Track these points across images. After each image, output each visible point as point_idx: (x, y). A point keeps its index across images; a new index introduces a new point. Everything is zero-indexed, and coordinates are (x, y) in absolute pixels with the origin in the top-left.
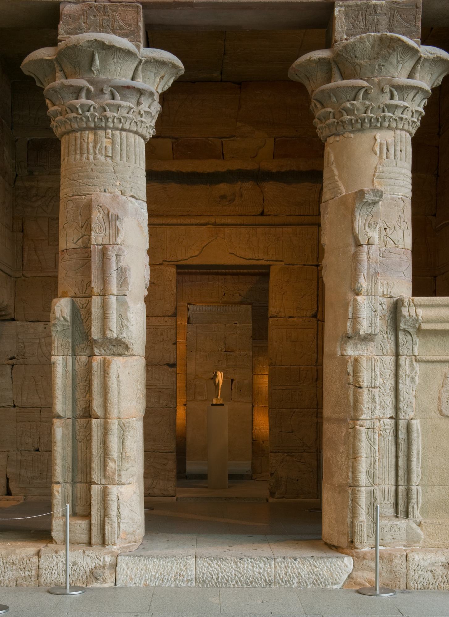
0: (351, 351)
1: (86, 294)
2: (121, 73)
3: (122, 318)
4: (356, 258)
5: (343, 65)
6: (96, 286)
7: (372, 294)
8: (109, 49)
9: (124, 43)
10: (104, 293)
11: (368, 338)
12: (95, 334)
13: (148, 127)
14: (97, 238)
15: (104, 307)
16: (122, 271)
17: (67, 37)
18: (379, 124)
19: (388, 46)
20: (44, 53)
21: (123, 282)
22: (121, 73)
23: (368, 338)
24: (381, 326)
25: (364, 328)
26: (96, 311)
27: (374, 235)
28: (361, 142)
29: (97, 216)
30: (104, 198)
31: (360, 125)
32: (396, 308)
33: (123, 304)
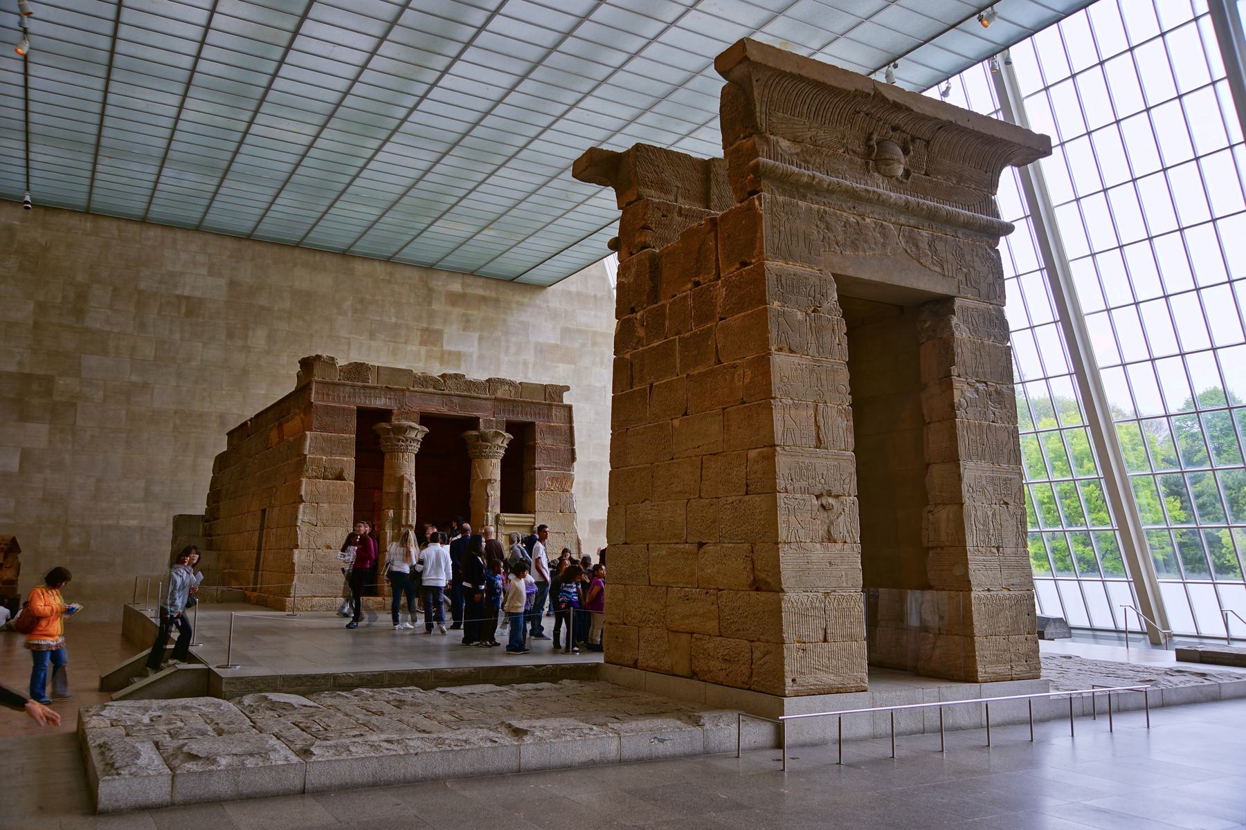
1: (400, 508)
2: (413, 435)
5: (483, 438)
8: (412, 428)
9: (414, 424)
12: (404, 522)
15: (408, 514)
17: (395, 422)
18: (493, 457)
19: (497, 434)
20: (384, 425)
22: (413, 435)
28: (487, 462)
31: (488, 457)
32: (497, 517)
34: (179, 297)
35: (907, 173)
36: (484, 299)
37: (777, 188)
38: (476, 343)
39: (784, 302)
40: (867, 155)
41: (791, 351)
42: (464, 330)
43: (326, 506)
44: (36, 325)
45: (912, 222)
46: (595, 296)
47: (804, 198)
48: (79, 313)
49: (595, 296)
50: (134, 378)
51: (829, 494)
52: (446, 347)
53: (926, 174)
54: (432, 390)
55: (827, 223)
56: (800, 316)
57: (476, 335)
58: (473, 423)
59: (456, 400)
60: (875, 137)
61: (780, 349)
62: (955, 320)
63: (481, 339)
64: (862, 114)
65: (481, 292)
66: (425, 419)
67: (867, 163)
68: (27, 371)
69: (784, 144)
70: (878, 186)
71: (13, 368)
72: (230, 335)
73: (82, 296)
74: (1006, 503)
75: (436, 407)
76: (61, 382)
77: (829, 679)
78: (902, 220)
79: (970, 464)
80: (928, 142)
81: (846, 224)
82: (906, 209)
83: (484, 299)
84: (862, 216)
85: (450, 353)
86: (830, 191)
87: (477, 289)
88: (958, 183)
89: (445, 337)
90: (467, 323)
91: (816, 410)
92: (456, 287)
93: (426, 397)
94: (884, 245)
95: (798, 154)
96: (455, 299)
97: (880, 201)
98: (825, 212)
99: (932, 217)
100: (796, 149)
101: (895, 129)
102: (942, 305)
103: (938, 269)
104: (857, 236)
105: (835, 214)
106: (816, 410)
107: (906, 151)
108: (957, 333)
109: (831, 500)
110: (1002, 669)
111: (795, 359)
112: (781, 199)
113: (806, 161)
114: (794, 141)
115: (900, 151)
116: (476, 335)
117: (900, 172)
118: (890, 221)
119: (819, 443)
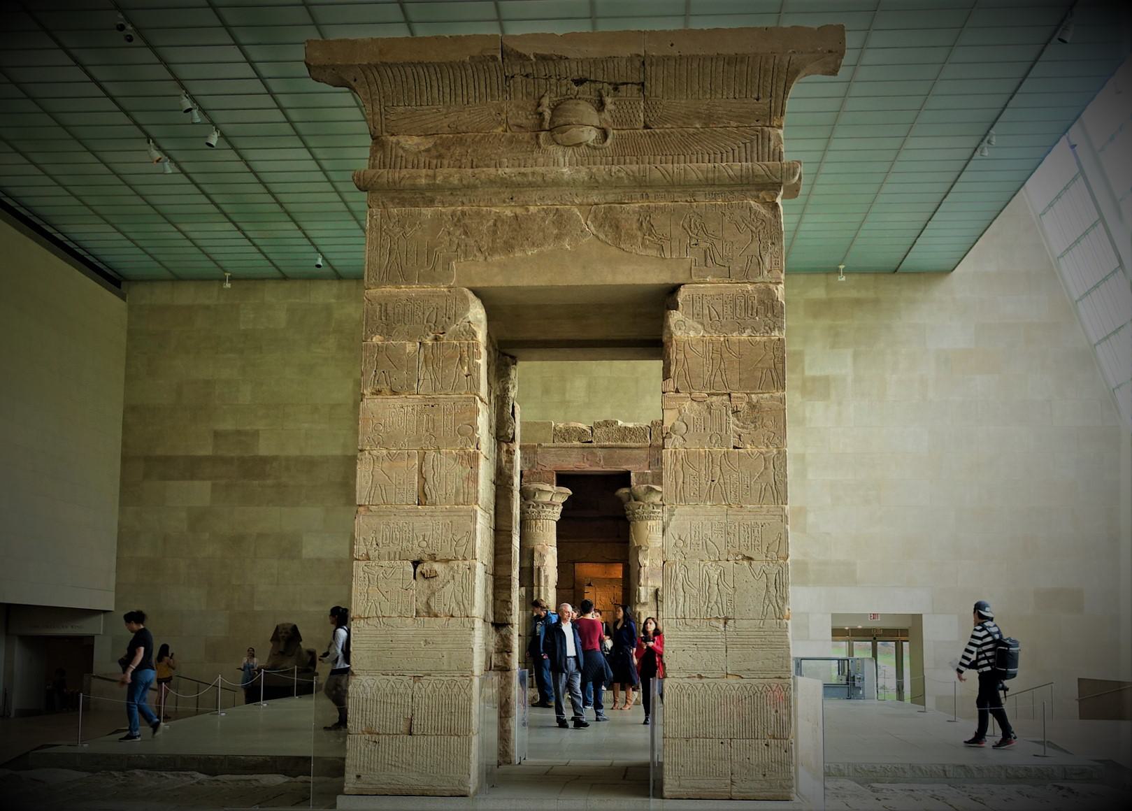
0: (638, 609)
3: (546, 595)
4: (639, 572)
6: (535, 582)
7: (646, 586)
9: (547, 487)
10: (539, 585)
11: (645, 604)
13: (557, 517)
14: (536, 564)
15: (539, 591)
16: (546, 577)
18: (650, 518)
21: (546, 581)
23: (645, 604)
24: (650, 599)
25: (643, 600)
26: (535, 593)
27: (647, 563)
29: (536, 555)
30: (539, 547)
31: (642, 519)
33: (546, 590)
35: (605, 134)
36: (858, 302)
37: (392, 199)
38: (849, 360)
39: (388, 334)
41: (394, 393)
42: (833, 347)
45: (610, 198)
47: (431, 202)
51: (433, 558)
53: (646, 127)
54: (576, 443)
55: (466, 225)
56: (410, 347)
57: (848, 353)
58: (623, 479)
59: (600, 453)
60: (546, 101)
61: (379, 392)
62: (675, 317)
63: (856, 356)
64: (518, 79)
66: (563, 479)
67: (537, 137)
69: (411, 142)
71: (337, 452)
72: (546, 391)
74: (750, 559)
75: (575, 463)
78: (594, 197)
80: (643, 84)
81: (498, 220)
83: (858, 302)
84: (525, 205)
85: (814, 379)
88: (706, 125)
89: (807, 359)
90: (835, 338)
91: (423, 459)
93: (563, 451)
94: (558, 237)
95: (428, 150)
97: (557, 183)
98: (464, 213)
100: (428, 143)
101: (579, 82)
102: (667, 296)
103: (654, 253)
104: (513, 235)
105: (478, 213)
106: (423, 459)
107: (601, 106)
108: (678, 334)
109: (437, 567)
111: (395, 401)
113: (440, 156)
115: (587, 111)
116: (848, 353)
117: (590, 135)
118: (573, 203)
119: (423, 499)
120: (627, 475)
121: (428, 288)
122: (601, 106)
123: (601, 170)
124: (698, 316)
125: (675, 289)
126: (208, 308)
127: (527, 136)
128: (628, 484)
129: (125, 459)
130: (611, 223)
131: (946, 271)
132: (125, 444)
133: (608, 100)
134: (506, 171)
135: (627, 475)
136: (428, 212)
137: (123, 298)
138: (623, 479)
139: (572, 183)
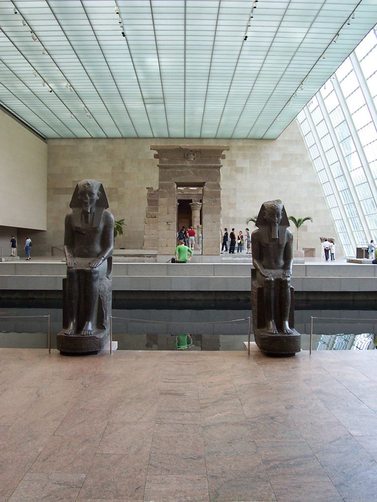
28: (194, 211)
31: (195, 210)
32: (198, 226)
34: (150, 160)
35: (194, 159)
36: (251, 147)
38: (248, 163)
39: (162, 189)
40: (184, 157)
43: (151, 224)
44: (113, 174)
46: (296, 141)
48: (123, 168)
49: (296, 141)
50: (139, 186)
52: (237, 166)
56: (166, 191)
58: (191, 201)
60: (186, 154)
63: (250, 162)
65: (250, 144)
68: (111, 187)
69: (165, 159)
70: (188, 164)
73: (123, 163)
76: (120, 189)
77: (167, 253)
79: (205, 215)
82: (193, 167)
83: (251, 147)
85: (239, 168)
86: (174, 167)
87: (248, 144)
90: (245, 157)
92: (240, 144)
96: (240, 148)
97: (188, 166)
99: (200, 167)
100: (168, 159)
107: (194, 155)
110: (210, 254)
112: (163, 170)
114: (167, 158)
116: (248, 161)
117: (192, 159)
119: (168, 213)
120: (192, 200)
121: (168, 182)
122: (194, 155)
123: (194, 165)
124: (208, 187)
125: (205, 183)
126: (69, 146)
127: (183, 159)
128: (192, 202)
129: (48, 189)
130: (195, 172)
131: (274, 139)
132: (48, 184)
133: (195, 154)
134: (180, 164)
135: (192, 200)
136: (168, 170)
137: (46, 143)
138: (191, 201)
139: (190, 167)
